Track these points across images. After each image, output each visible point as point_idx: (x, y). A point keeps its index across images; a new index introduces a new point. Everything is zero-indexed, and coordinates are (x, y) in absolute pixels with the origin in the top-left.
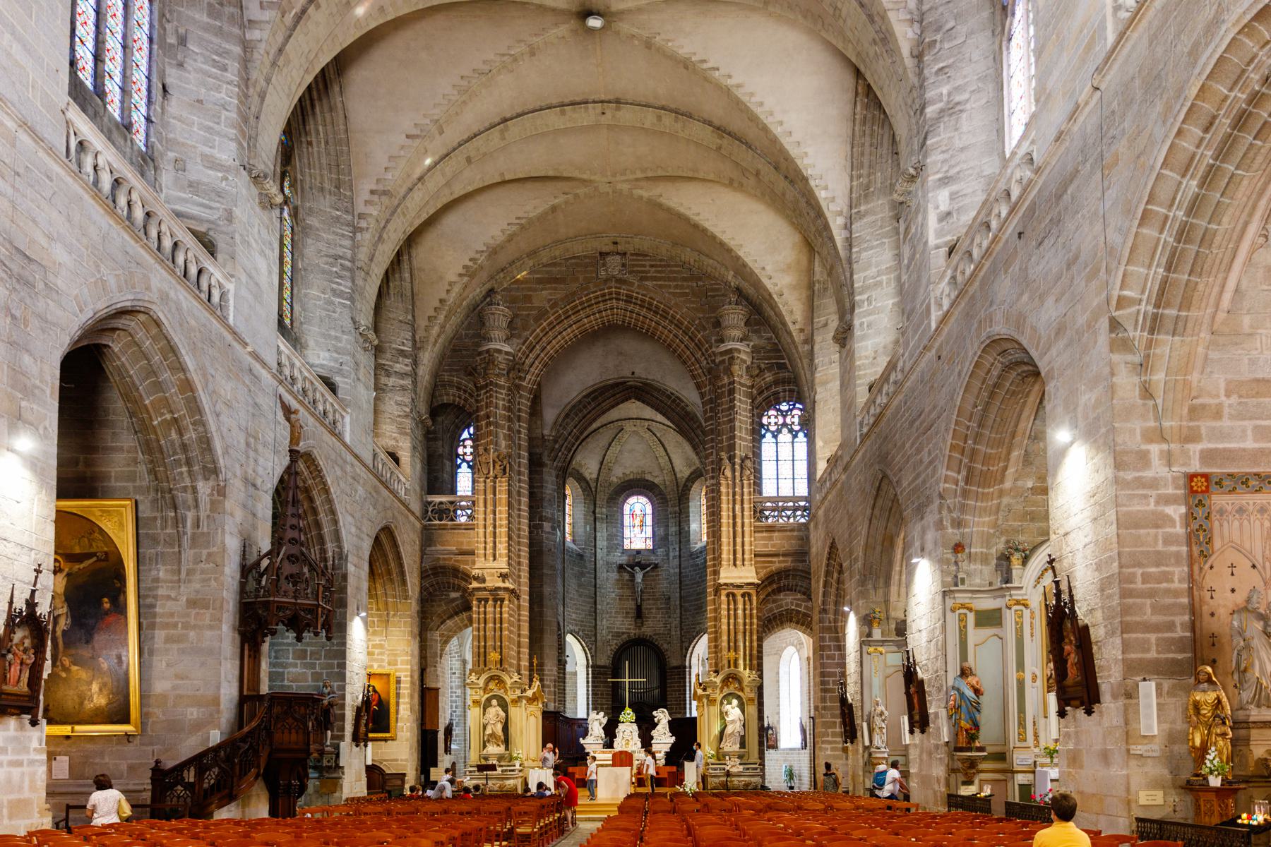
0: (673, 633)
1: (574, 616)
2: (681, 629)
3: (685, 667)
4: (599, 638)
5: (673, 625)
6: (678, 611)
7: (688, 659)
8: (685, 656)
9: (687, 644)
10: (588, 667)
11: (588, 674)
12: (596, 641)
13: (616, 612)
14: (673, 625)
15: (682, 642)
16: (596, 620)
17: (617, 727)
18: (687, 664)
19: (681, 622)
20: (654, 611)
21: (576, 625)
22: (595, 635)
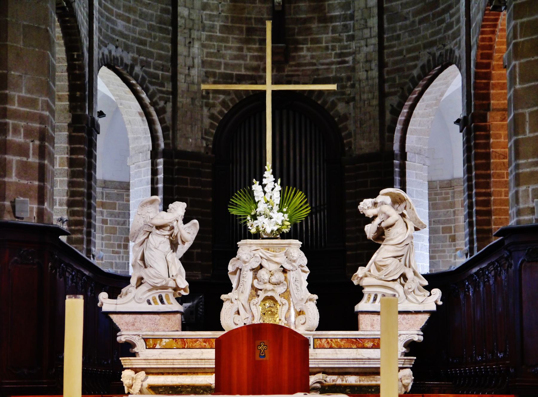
0: (362, 75)
1: (121, 25)
2: (382, 65)
3: (392, 155)
4: (182, 85)
5: (361, 57)
6: (374, 22)
7: (397, 135)
8: (392, 130)
9: (393, 100)
10: (154, 154)
11: (154, 172)
12: (174, 92)
13: (225, 29)
14: (361, 57)
15: (383, 96)
16: (174, 42)
17: (233, 252)
18: (396, 147)
19: (381, 47)
20: (314, 26)
21: (127, 48)
22: (174, 79)
